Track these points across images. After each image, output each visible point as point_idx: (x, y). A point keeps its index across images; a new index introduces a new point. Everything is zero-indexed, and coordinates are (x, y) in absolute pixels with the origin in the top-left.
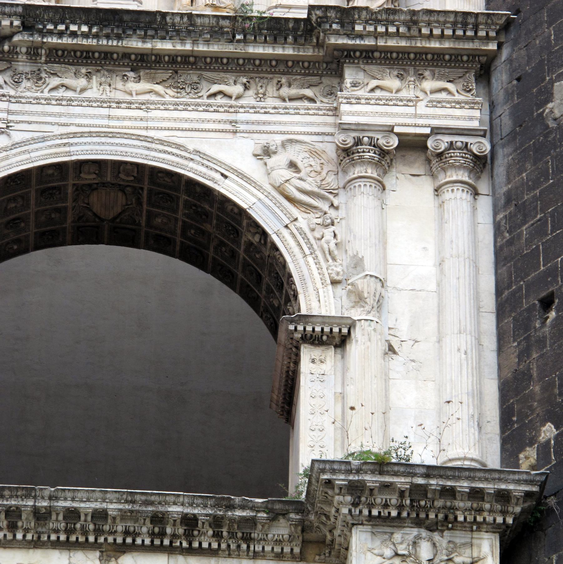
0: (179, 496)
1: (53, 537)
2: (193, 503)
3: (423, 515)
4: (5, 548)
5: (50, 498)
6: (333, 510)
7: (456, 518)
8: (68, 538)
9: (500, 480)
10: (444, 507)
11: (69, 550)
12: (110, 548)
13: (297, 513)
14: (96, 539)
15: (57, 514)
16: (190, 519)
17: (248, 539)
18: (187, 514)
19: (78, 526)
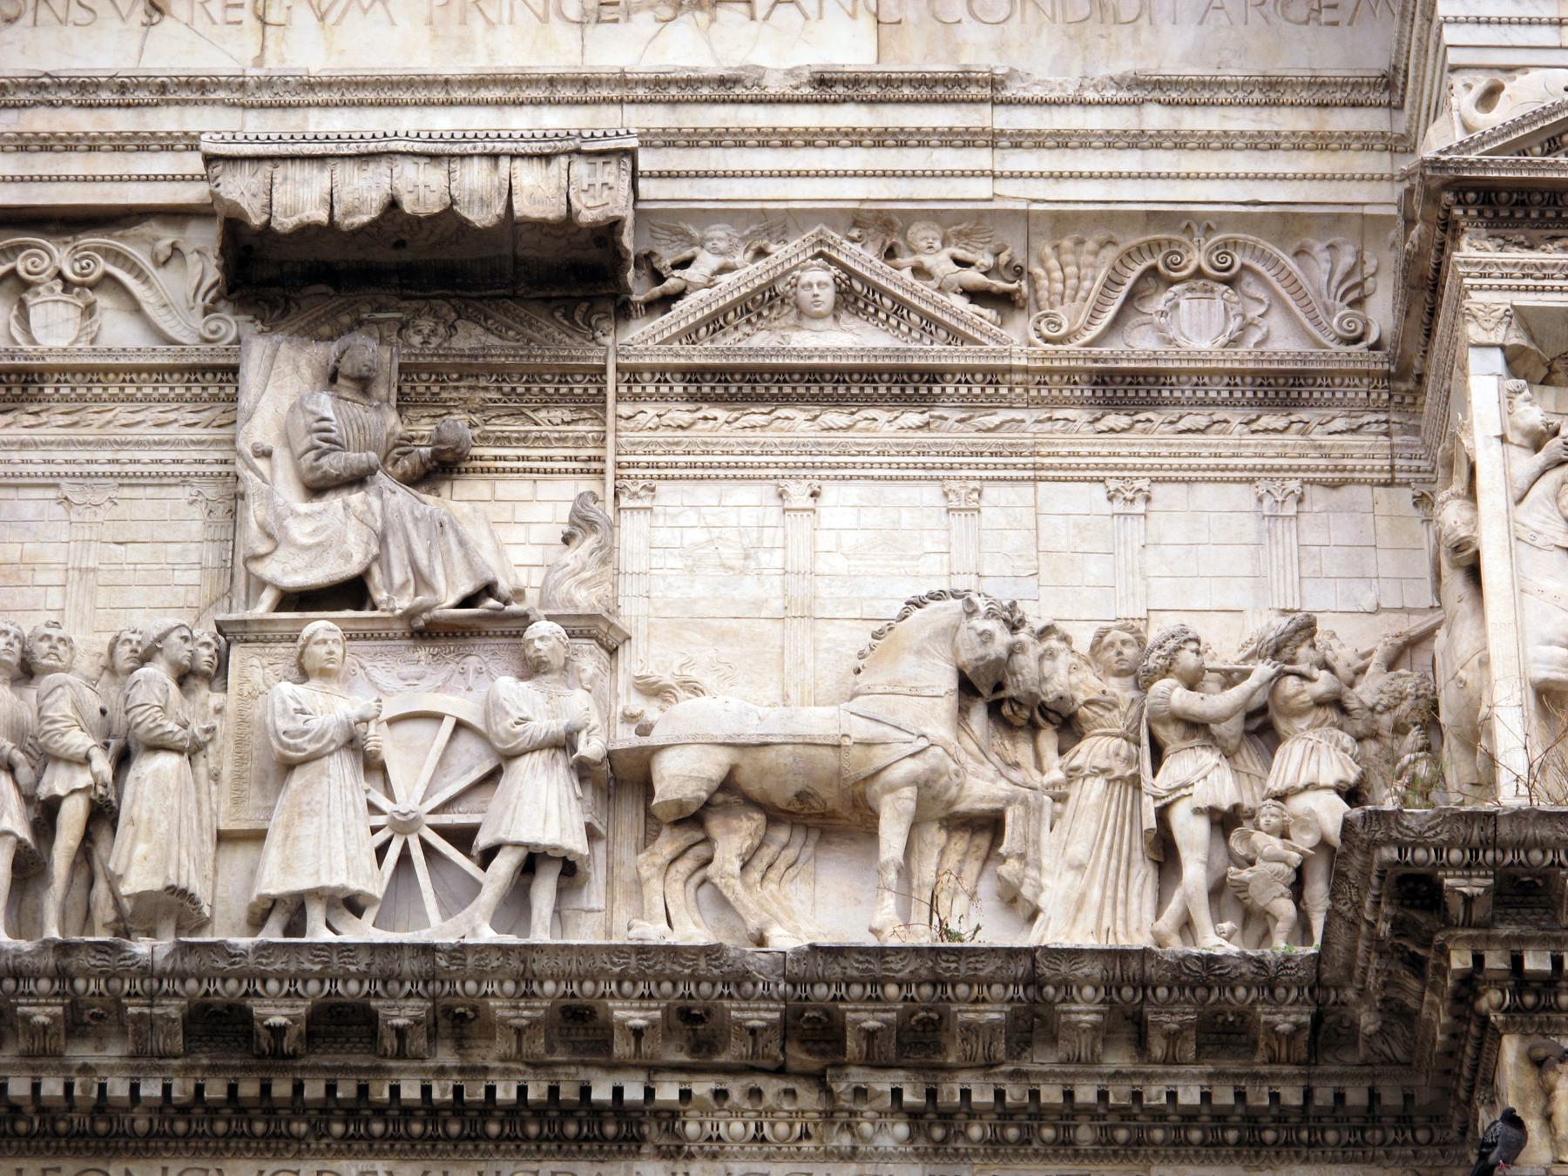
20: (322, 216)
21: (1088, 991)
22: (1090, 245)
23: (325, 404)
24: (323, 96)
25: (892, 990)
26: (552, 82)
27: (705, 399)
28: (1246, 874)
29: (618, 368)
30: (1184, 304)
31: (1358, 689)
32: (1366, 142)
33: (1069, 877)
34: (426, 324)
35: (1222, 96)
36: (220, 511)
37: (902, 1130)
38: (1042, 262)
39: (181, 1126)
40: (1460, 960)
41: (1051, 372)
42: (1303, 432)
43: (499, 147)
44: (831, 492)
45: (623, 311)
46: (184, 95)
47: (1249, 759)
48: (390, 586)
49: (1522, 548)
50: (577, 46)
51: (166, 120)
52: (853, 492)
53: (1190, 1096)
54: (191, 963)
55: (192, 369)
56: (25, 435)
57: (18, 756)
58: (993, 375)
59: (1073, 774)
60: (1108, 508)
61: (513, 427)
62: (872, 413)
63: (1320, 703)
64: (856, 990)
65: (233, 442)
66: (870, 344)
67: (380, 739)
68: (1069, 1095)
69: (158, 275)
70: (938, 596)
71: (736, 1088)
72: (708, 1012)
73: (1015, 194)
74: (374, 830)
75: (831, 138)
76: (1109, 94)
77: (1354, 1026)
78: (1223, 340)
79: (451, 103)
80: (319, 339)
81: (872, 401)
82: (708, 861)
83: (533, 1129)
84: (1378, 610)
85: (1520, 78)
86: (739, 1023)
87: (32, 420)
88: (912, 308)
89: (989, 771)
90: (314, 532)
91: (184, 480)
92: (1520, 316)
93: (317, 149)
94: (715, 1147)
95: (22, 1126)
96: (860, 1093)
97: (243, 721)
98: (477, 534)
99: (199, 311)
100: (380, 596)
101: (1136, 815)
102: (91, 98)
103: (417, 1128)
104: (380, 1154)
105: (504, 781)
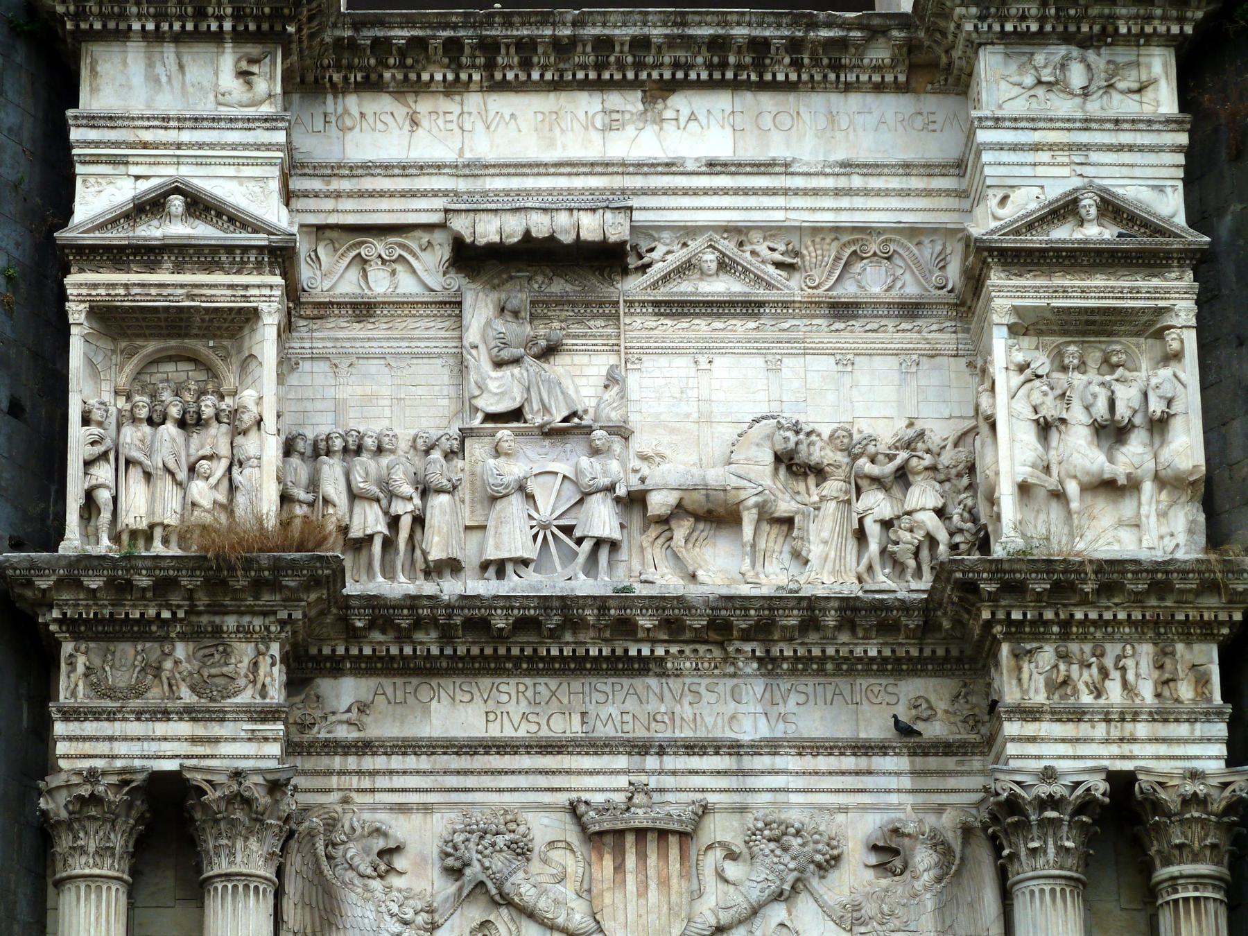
0: (743, 14)
1: (580, 75)
2: (763, 22)
3: (1072, 28)
4: (517, 92)
5: (574, 24)
6: (952, 26)
7: (1117, 29)
8: (599, 76)
10: (1101, 16)
11: (602, 91)
12: (654, 86)
13: (901, 30)
14: (636, 76)
15: (584, 46)
16: (759, 43)
17: (837, 67)
18: (755, 38)
19: (612, 59)
20: (497, 239)
21: (833, 612)
22: (828, 240)
23: (499, 325)
24: (492, 171)
25: (752, 612)
26: (592, 164)
27: (662, 315)
28: (895, 548)
29: (625, 301)
30: (868, 269)
31: (942, 458)
32: (948, 193)
33: (821, 546)
34: (540, 278)
35: (886, 171)
36: (456, 370)
37: (755, 665)
38: (807, 248)
39: (460, 665)
40: (986, 615)
41: (811, 303)
42: (919, 332)
44: (718, 360)
45: (625, 272)
46: (431, 171)
47: (896, 491)
48: (532, 411)
49: (1014, 420)
50: (601, 141)
51: (424, 183)
53: (873, 652)
55: (441, 303)
56: (369, 334)
57: (381, 495)
58: (786, 304)
59: (823, 499)
60: (835, 368)
63: (927, 469)
64: (738, 612)
65: (461, 338)
67: (532, 486)
68: (823, 651)
69: (422, 255)
70: (764, 418)
71: (688, 649)
72: (677, 620)
73: (796, 218)
74: (532, 527)
75: (716, 192)
76: (837, 170)
77: (940, 625)
78: (885, 287)
79: (548, 174)
80: (494, 288)
81: (734, 316)
82: (671, 538)
83: (605, 666)
84: (951, 417)
85: (1017, 192)
86: (690, 626)
87: (371, 326)
88: (751, 272)
89: (787, 497)
90: (499, 387)
91: (439, 356)
92: (1016, 310)
93: (493, 206)
94: (678, 673)
95: (395, 666)
96: (738, 651)
97: (473, 474)
98: (567, 383)
99: (441, 273)
100: (529, 416)
101: (849, 518)
102: (390, 172)
103: (557, 666)
104: (542, 676)
105: (585, 506)
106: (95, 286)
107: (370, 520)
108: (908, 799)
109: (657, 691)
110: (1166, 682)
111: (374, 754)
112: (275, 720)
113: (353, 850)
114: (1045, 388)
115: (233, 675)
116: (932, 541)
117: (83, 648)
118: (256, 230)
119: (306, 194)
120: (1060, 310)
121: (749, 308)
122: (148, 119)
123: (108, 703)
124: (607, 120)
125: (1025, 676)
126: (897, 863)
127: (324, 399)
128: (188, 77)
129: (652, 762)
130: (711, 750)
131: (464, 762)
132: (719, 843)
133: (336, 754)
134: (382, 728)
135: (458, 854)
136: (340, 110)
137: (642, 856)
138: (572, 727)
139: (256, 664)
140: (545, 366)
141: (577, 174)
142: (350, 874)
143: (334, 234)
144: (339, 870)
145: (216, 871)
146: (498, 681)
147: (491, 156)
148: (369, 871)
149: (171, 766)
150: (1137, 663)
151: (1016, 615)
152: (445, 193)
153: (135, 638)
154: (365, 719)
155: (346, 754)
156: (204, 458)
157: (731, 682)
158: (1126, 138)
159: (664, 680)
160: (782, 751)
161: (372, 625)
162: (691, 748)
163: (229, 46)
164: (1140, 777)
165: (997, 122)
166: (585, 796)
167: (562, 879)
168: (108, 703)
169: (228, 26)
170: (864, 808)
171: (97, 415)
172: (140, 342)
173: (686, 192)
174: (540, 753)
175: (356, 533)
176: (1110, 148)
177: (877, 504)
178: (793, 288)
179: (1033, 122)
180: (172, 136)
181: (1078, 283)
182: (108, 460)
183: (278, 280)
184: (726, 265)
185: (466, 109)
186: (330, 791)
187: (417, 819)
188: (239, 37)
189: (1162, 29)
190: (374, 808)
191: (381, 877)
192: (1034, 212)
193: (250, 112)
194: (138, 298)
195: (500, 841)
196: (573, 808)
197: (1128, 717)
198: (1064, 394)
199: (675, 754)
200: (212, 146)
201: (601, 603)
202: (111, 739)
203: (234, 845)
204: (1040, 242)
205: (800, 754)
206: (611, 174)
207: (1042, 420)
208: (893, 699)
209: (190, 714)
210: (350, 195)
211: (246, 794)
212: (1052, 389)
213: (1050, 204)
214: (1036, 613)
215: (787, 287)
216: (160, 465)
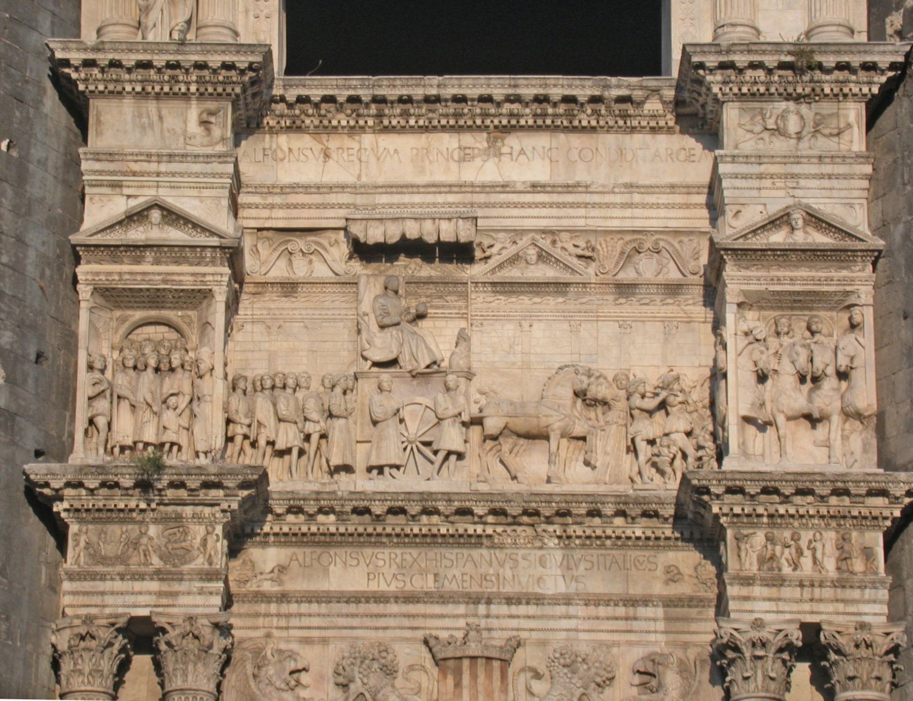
9: (865, 52)
17: (625, 116)
20: (383, 241)
24: (380, 190)
25: (554, 504)
26: (450, 186)
27: (497, 292)
42: (678, 305)
43: (436, 216)
46: (336, 190)
51: (332, 198)
52: (542, 325)
53: (639, 533)
54: (354, 496)
55: (343, 283)
56: (293, 306)
58: (584, 284)
61: (440, 302)
62: (549, 298)
63: (680, 403)
64: (544, 504)
65: (356, 308)
66: (548, 275)
67: (404, 413)
69: (332, 249)
73: (593, 224)
74: (403, 442)
75: (536, 205)
76: (623, 190)
81: (548, 294)
87: (294, 300)
92: (744, 293)
94: (501, 547)
98: (430, 341)
99: (344, 263)
100: (402, 364)
102: (309, 190)
106: (98, 274)
107: (288, 437)
108: (661, 638)
109: (488, 559)
110: (846, 559)
111: (289, 602)
112: (218, 580)
113: (271, 670)
114: (763, 348)
115: (189, 548)
116: (685, 456)
117: (84, 529)
118: (213, 234)
119: (250, 206)
120: (774, 293)
121: (560, 287)
122: (137, 155)
123: (100, 568)
124: (462, 154)
125: (743, 554)
126: (654, 683)
127: (260, 351)
128: (165, 125)
129: (482, 609)
130: (524, 601)
131: (352, 608)
132: (529, 667)
133: (262, 601)
134: (295, 584)
135: (346, 673)
136: (274, 146)
137: (474, 676)
138: (430, 584)
139: (205, 540)
140: (415, 329)
141: (440, 193)
142: (270, 688)
143: (270, 234)
144: (262, 686)
145: (174, 686)
146: (376, 551)
147: (381, 181)
148: (283, 686)
149: (143, 612)
150: (824, 546)
151: (737, 510)
152: (348, 206)
153: (123, 521)
154: (285, 578)
155: (269, 602)
156: (172, 395)
157: (539, 553)
158: (827, 169)
159: (492, 551)
160: (573, 602)
161: (289, 511)
162: (510, 600)
163: (194, 103)
164: (824, 627)
165: (734, 159)
166: (434, 633)
167: (418, 692)
168: (100, 568)
169: (193, 88)
170: (630, 643)
171: (98, 365)
172: (130, 312)
173: (516, 205)
174: (405, 602)
175: (280, 445)
176: (815, 176)
177: (647, 428)
178: (590, 272)
179: (759, 159)
180: (153, 167)
181: (788, 274)
182: (105, 397)
183: (227, 270)
184: (543, 257)
185: (363, 146)
186: (257, 628)
187: (317, 649)
188: (201, 96)
189: (856, 90)
190: (288, 640)
191: (292, 690)
192: (757, 223)
193: (209, 151)
194: (128, 282)
195: (376, 665)
196: (426, 642)
197: (816, 584)
198: (777, 352)
199: (499, 603)
200: (182, 174)
201: (448, 497)
202: (103, 593)
203: (187, 669)
204: (761, 244)
205: (586, 605)
206: (464, 192)
207: (760, 371)
208: (654, 567)
209: (159, 575)
210: (281, 207)
211: (196, 632)
212: (767, 349)
213: (769, 217)
214: (751, 509)
215: (586, 273)
216: (142, 400)
